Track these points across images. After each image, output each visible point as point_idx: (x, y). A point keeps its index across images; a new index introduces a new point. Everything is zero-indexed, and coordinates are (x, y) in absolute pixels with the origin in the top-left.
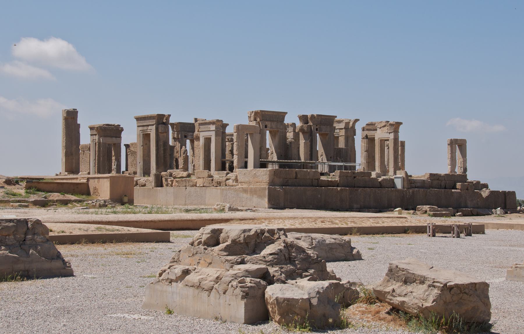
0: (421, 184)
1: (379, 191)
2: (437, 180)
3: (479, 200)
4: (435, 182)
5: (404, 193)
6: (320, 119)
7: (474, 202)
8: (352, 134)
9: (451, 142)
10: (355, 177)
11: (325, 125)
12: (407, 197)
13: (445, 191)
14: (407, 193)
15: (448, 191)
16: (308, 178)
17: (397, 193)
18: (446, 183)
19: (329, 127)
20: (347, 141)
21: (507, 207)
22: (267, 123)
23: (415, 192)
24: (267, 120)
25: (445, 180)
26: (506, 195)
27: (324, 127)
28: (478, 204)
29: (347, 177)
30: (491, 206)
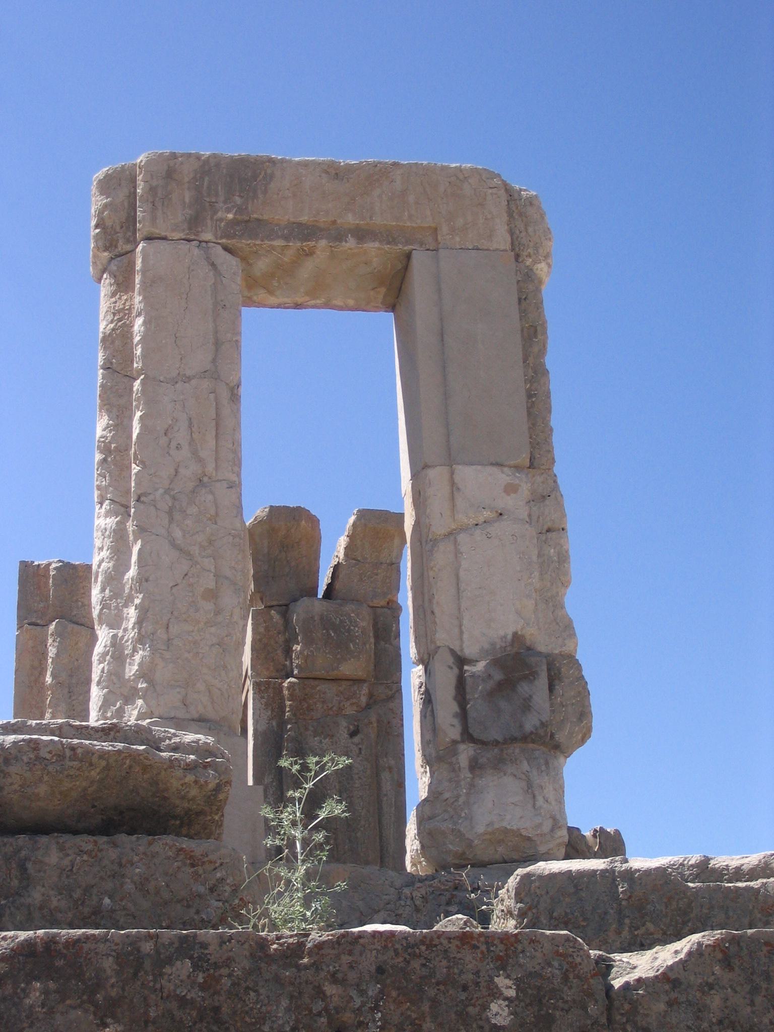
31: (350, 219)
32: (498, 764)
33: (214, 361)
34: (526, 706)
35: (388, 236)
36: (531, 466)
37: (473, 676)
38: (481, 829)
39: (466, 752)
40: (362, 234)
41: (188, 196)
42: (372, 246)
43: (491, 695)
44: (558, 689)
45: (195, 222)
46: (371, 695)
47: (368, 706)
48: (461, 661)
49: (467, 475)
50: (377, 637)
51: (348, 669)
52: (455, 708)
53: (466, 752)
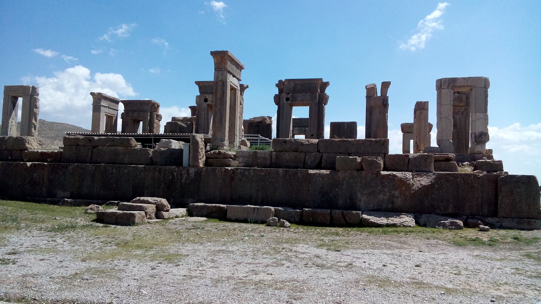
0: (246, 159)
1: (114, 170)
2: (294, 151)
3: (397, 193)
4: (287, 156)
5: (176, 174)
6: (292, 85)
7: (381, 197)
8: (379, 103)
9: (439, 86)
10: (95, 147)
11: (302, 93)
12: (181, 182)
13: (286, 172)
14: (181, 175)
15: (297, 173)
16: (4, 148)
17: (157, 173)
18: (322, 156)
19: (309, 94)
20: (371, 115)
21: (499, 215)
22: (207, 96)
23: (203, 174)
24: (206, 93)
25: (318, 151)
26: (500, 184)
27: (300, 95)
28: (393, 203)
29: (78, 147)
30: (442, 208)
31: (466, 85)
32: (479, 144)
33: (450, 103)
34: (482, 138)
35: (470, 86)
36: (485, 112)
37: (477, 136)
38: (476, 151)
39: (475, 143)
40: (467, 86)
41: (447, 83)
42: (468, 88)
43: (478, 138)
44: (486, 136)
45: (448, 87)
46: (465, 108)
47: (465, 110)
48: (475, 134)
49: (477, 114)
50: (467, 99)
51: (461, 105)
52: (474, 138)
53: (475, 143)
